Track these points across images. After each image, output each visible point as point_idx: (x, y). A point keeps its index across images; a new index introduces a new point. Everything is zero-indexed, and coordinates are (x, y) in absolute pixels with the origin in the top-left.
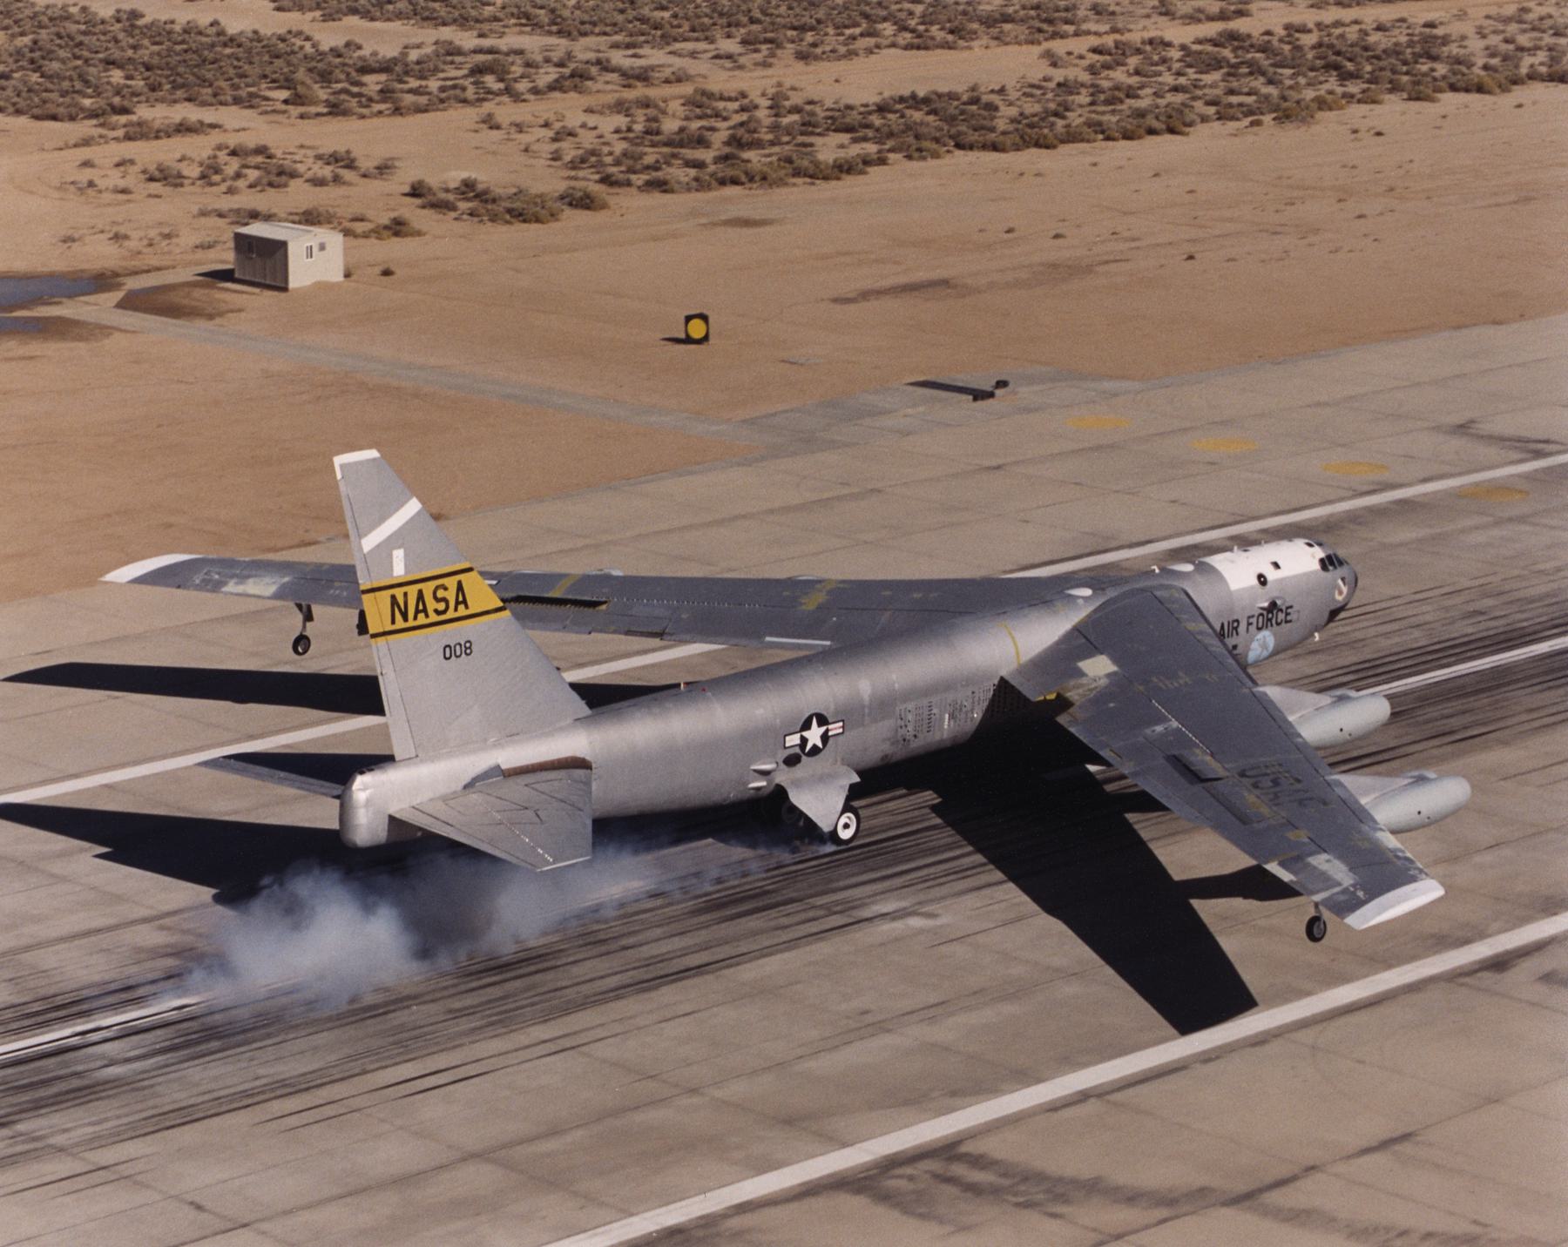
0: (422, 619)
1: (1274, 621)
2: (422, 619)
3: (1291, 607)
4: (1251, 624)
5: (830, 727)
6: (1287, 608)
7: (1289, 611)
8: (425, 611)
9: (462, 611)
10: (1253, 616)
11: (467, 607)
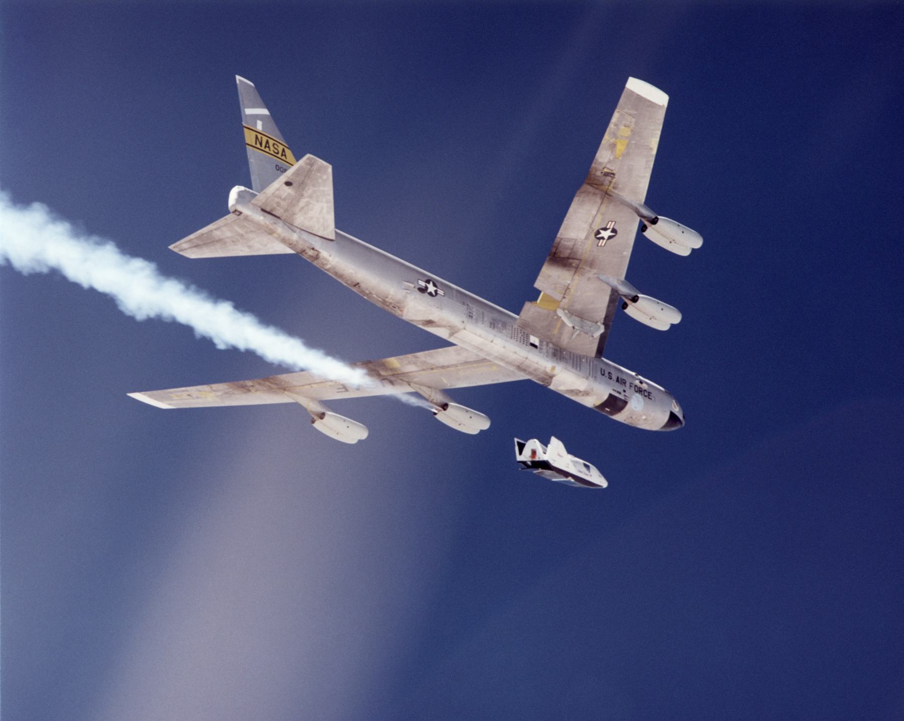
0: (267, 150)
1: (643, 393)
2: (267, 150)
5: (438, 290)
6: (649, 392)
8: (269, 147)
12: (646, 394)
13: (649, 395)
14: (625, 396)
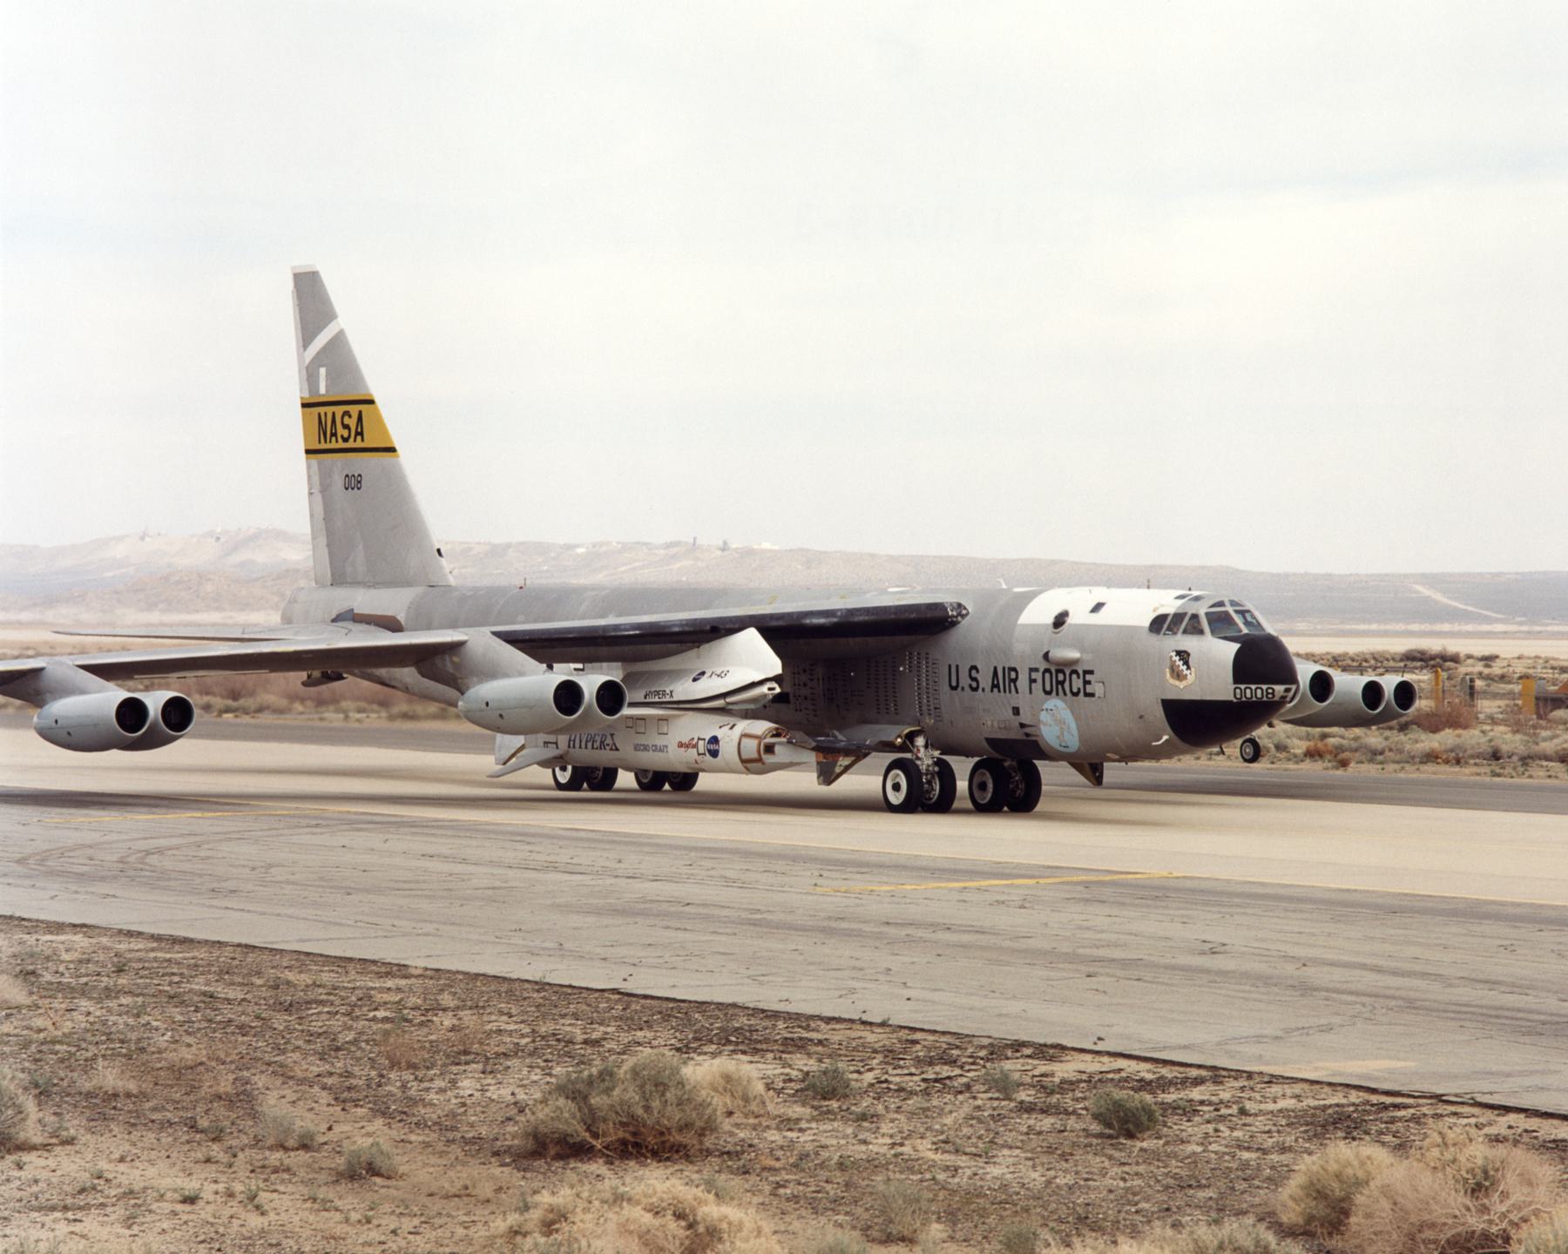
1: (1067, 685)
3: (1091, 672)
4: (1034, 681)
6: (1086, 672)
7: (1088, 677)
9: (359, 444)
10: (1036, 670)
11: (363, 440)
12: (1077, 683)
13: (1086, 682)
14: (1022, 726)
